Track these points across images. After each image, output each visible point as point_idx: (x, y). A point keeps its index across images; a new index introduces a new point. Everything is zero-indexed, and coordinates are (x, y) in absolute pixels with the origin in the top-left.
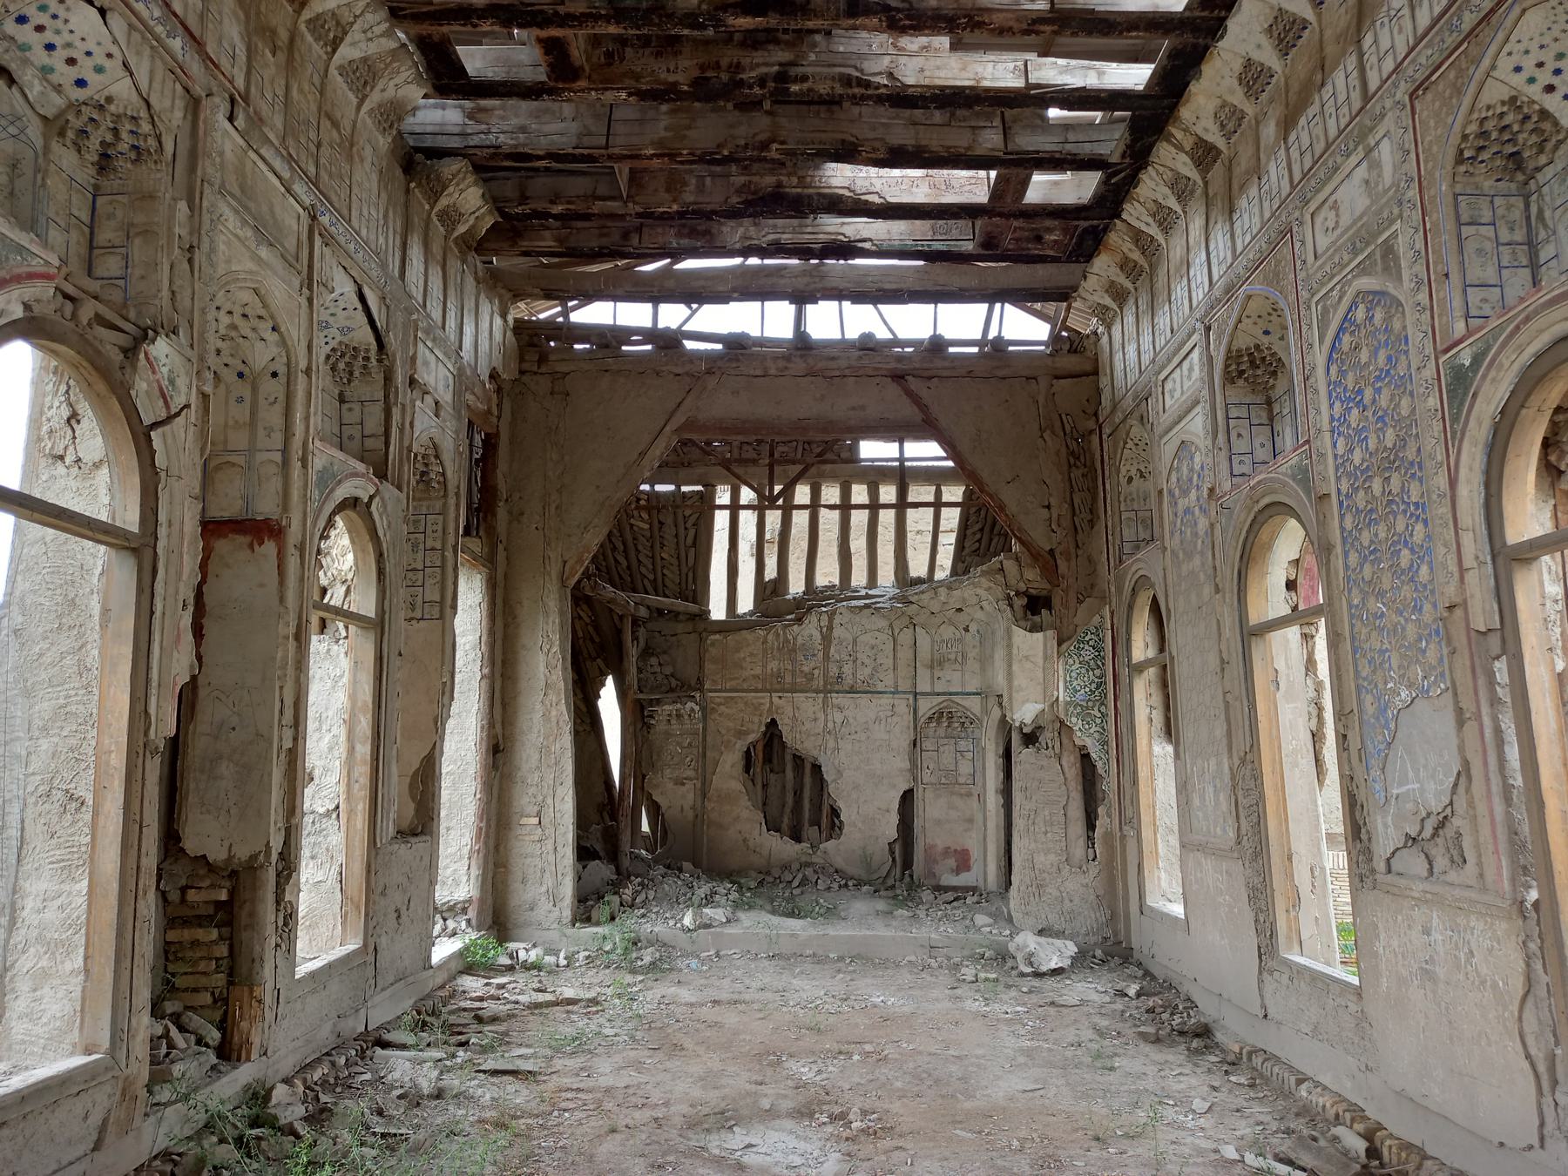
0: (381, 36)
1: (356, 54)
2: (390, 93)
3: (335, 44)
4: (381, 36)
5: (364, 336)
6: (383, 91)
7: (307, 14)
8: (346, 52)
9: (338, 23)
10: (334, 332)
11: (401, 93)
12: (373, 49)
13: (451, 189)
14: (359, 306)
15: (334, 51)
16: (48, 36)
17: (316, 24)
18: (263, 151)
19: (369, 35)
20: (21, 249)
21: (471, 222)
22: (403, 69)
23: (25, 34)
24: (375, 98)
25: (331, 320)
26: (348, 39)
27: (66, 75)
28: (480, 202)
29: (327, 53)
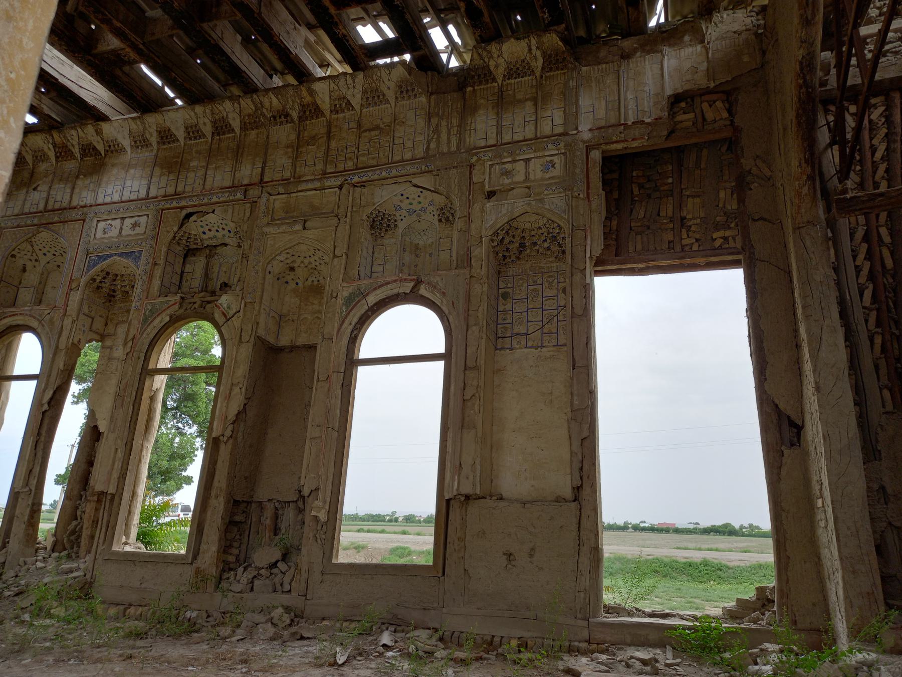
0: (354, 81)
1: (359, 96)
2: (392, 85)
3: (349, 104)
4: (354, 81)
5: (440, 200)
6: (389, 88)
7: (327, 113)
8: (356, 102)
9: (339, 99)
10: (430, 209)
11: (395, 79)
12: (359, 88)
13: (492, 64)
14: (421, 190)
15: (353, 107)
16: (214, 229)
17: (335, 110)
18: (300, 189)
19: (351, 86)
20: (167, 302)
21: (539, 54)
22: (379, 74)
23: (211, 234)
24: (390, 95)
25: (422, 205)
26: (349, 98)
27: (226, 232)
28: (523, 44)
29: (352, 110)
